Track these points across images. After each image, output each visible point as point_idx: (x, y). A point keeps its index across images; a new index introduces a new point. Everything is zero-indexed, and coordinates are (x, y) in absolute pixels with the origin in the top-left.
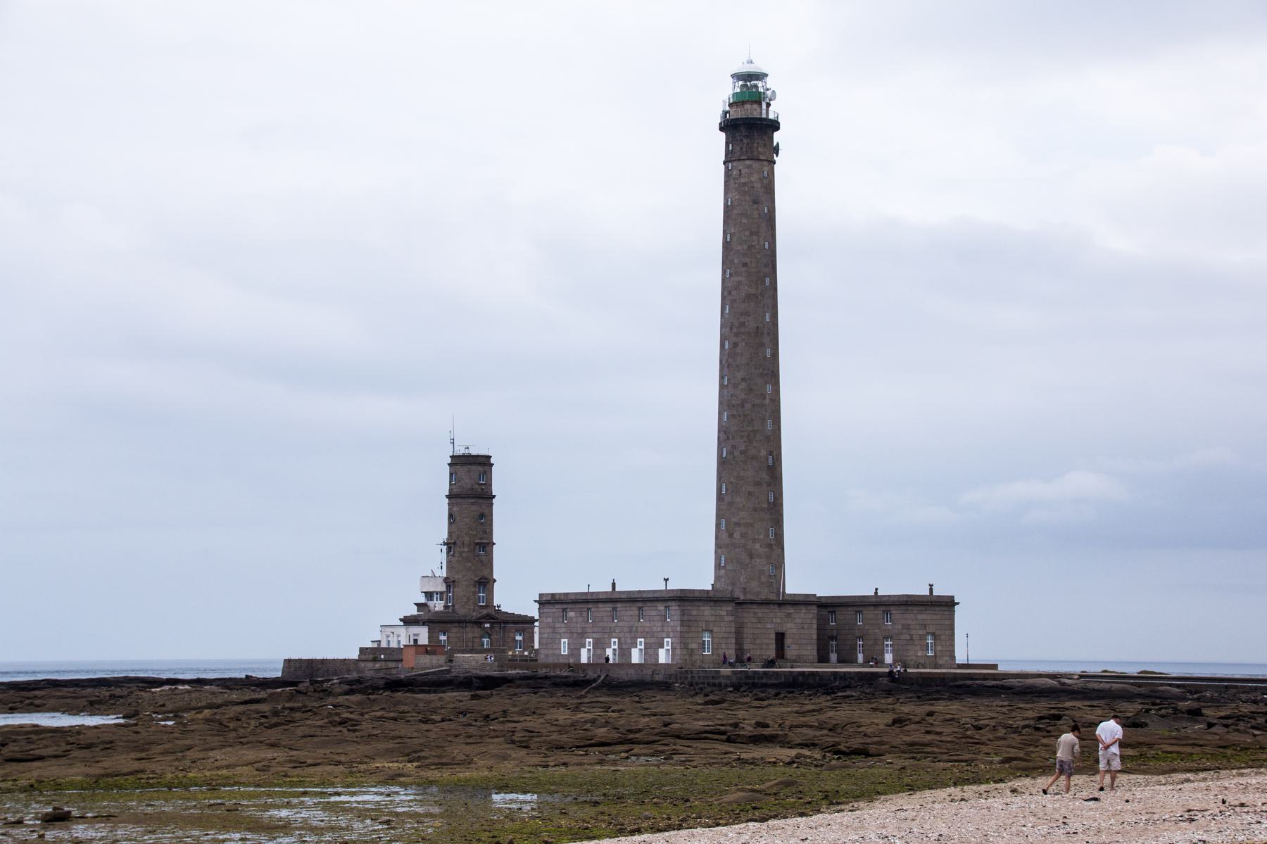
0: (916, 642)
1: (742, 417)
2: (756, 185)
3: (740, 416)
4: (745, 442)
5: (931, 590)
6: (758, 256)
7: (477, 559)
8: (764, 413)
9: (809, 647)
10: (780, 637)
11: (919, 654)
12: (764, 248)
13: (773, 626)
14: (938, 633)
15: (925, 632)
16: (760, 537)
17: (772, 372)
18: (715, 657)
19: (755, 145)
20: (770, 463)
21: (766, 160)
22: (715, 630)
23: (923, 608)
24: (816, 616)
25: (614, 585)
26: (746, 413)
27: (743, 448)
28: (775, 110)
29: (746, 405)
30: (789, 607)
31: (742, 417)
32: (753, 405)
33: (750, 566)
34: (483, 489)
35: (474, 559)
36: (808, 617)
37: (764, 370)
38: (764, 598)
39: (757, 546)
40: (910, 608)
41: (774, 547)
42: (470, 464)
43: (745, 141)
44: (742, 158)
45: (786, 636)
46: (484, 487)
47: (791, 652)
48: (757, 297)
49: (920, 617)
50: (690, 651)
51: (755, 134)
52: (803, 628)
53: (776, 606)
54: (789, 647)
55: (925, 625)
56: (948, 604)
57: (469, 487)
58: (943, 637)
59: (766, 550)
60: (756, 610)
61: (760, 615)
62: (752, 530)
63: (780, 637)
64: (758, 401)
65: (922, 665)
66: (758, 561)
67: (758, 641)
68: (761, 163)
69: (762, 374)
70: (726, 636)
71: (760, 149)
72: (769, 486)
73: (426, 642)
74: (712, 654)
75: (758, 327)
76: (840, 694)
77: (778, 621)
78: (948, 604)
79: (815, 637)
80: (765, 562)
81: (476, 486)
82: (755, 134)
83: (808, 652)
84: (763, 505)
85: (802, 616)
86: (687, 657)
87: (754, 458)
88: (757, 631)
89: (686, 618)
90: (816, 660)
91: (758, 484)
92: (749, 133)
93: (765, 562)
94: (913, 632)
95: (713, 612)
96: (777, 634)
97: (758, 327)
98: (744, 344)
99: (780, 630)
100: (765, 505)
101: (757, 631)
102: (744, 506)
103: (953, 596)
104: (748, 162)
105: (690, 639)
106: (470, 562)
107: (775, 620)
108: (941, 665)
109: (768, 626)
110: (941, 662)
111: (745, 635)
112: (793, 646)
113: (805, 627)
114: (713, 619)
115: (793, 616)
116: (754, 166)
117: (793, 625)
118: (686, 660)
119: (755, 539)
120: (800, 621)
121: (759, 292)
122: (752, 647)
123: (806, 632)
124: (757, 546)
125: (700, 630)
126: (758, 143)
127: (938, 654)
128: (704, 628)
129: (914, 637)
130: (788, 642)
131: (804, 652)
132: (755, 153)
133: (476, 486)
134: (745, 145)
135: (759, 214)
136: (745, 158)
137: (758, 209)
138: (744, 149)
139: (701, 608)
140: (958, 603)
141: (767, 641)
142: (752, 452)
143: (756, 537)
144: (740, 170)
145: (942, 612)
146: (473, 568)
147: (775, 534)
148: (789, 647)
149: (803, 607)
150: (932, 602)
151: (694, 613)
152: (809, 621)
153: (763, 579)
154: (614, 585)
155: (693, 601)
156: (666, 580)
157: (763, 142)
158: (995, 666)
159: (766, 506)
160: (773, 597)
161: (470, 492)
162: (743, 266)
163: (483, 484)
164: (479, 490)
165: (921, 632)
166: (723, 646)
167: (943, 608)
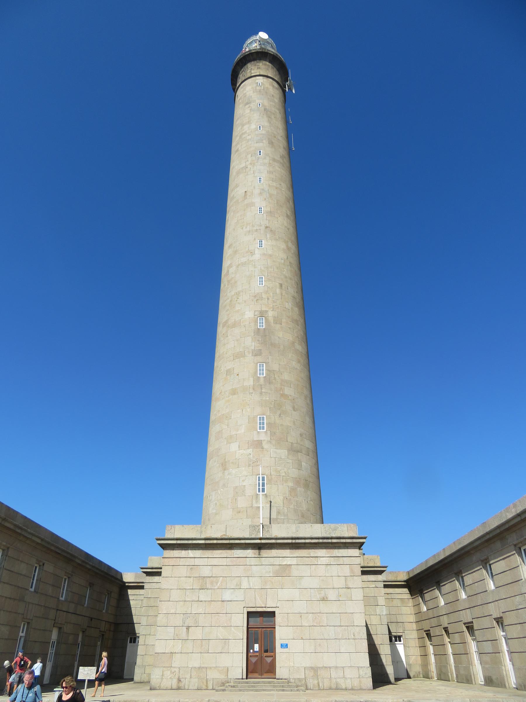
13: (239, 595)
16: (239, 432)
30: (287, 552)
37: (253, 226)
41: (266, 446)
45: (278, 619)
52: (324, 599)
53: (250, 552)
59: (250, 451)
60: (197, 562)
61: (206, 571)
67: (196, 633)
69: (249, 231)
72: (256, 355)
73: (258, 650)
77: (255, 583)
85: (321, 571)
88: (196, 609)
99: (260, 606)
100: (250, 382)
101: (196, 609)
109: (227, 595)
111: (161, 619)
115: (295, 572)
119: (231, 437)
120: (315, 583)
122: (178, 646)
123: (334, 608)
124: (234, 447)
131: (328, 660)
141: (221, 633)
152: (340, 583)
153: (242, 503)
159: (251, 382)
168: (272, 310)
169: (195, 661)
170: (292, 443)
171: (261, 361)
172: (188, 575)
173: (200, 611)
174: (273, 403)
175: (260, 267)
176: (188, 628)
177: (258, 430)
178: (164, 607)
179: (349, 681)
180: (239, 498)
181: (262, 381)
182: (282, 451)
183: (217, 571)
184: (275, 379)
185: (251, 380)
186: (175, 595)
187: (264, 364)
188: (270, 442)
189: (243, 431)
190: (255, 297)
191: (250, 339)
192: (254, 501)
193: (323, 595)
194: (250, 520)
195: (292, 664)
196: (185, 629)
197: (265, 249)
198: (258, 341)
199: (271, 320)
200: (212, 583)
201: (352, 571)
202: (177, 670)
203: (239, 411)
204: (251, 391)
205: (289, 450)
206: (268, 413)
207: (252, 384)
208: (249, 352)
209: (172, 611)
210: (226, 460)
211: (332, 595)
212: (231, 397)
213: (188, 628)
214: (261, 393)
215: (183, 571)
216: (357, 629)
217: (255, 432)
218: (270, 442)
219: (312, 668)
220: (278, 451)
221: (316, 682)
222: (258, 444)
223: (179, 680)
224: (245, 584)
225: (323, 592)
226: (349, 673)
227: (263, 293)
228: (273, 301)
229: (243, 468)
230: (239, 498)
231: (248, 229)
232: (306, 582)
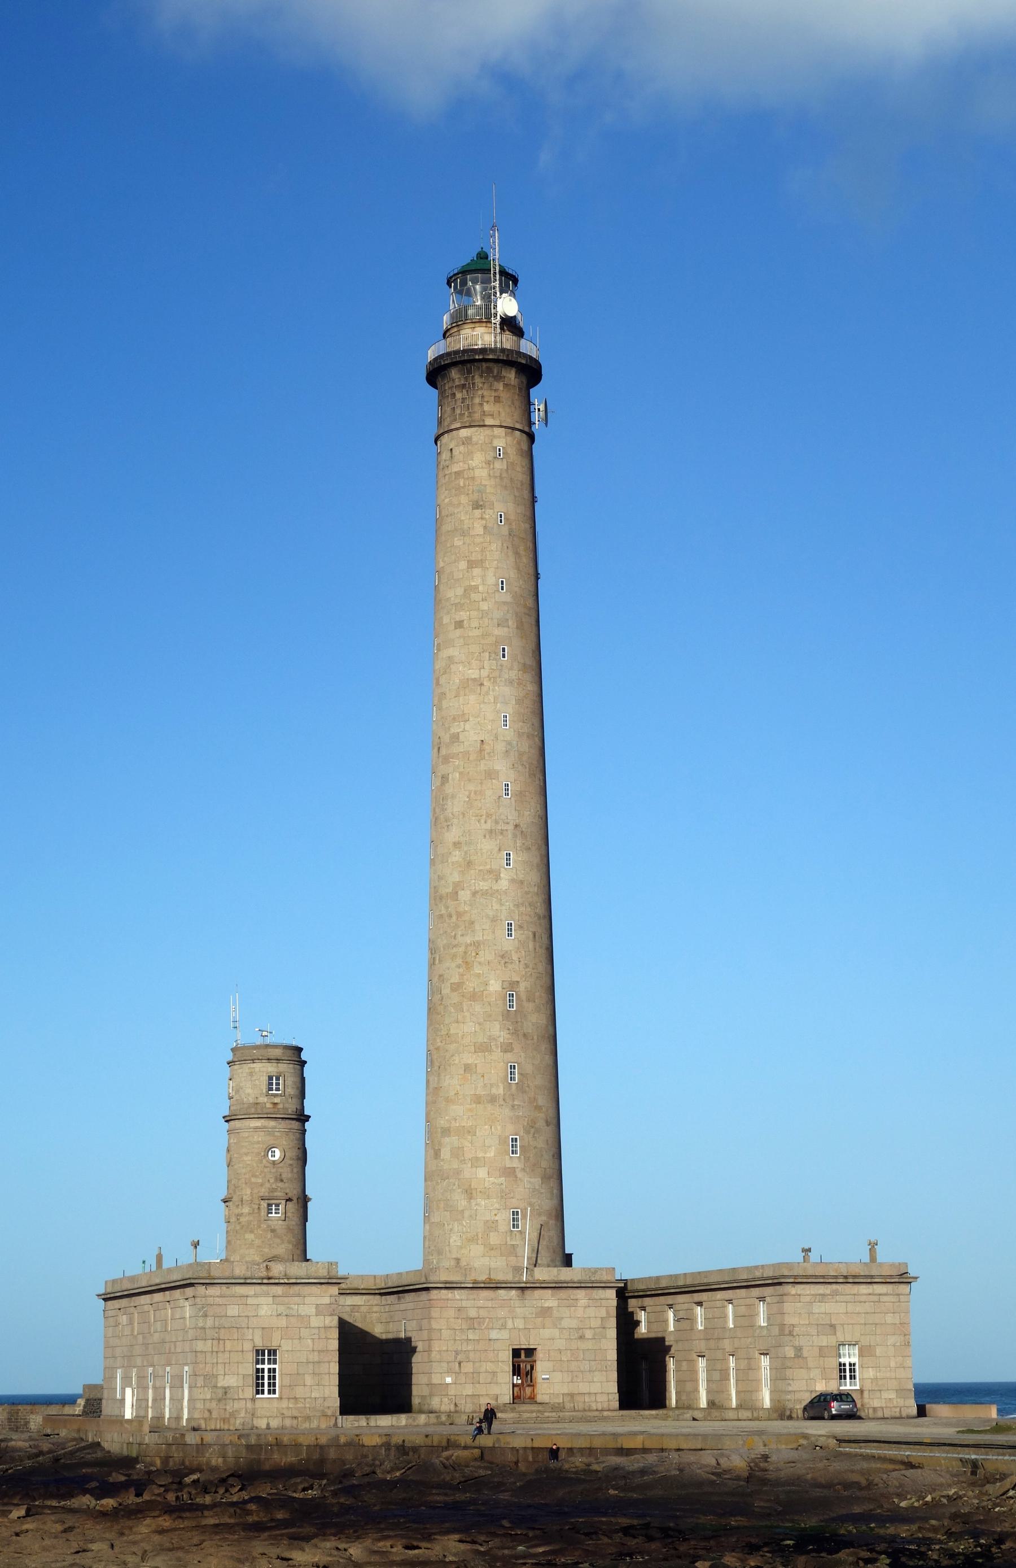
0: (811, 1364)
1: (454, 918)
2: (478, 473)
3: (450, 916)
4: (459, 966)
6: (484, 606)
7: (264, 1226)
8: (496, 906)
9: (598, 1377)
14: (865, 1341)
15: (832, 1341)
16: (488, 1155)
17: (516, 826)
18: (284, 1404)
19: (477, 400)
21: (501, 426)
22: (286, 1346)
25: (159, 1258)
26: (461, 909)
27: (455, 979)
29: (461, 893)
31: (454, 918)
32: (474, 894)
33: (467, 1214)
34: (275, 1104)
35: (259, 1227)
37: (497, 822)
39: (482, 1173)
41: (520, 1175)
42: (253, 1061)
43: (459, 396)
44: (453, 427)
45: (539, 1355)
46: (277, 1100)
48: (482, 685)
49: (818, 1308)
50: (220, 1392)
51: (478, 380)
52: (582, 1337)
55: (833, 1326)
57: (251, 1100)
58: (879, 1351)
60: (464, 1304)
61: (473, 1313)
62: (471, 1143)
64: (483, 885)
66: (483, 1203)
67: (468, 1368)
68: (488, 431)
69: (491, 831)
70: (316, 1359)
71: (486, 407)
72: (506, 1052)
74: (280, 1398)
76: (54, 1503)
77: (520, 1323)
79: (612, 1355)
80: (497, 1206)
81: (263, 1099)
82: (478, 380)
83: (595, 1388)
84: (494, 1091)
85: (580, 1312)
86: (214, 1404)
87: (474, 997)
89: (209, 1322)
90: (617, 1404)
91: (482, 1048)
92: (466, 379)
93: (497, 1206)
94: (802, 1341)
95: (281, 1309)
96: (516, 1353)
97: (482, 741)
98: (457, 775)
100: (500, 1091)
102: (457, 1094)
103: (906, 1265)
104: (464, 433)
105: (220, 1367)
106: (252, 1232)
108: (875, 1409)
109: (494, 1334)
110: (876, 1403)
112: (558, 1376)
113: (587, 1336)
114: (283, 1322)
115: (555, 1313)
116: (475, 439)
117: (556, 1332)
118: (210, 1411)
119: (477, 1159)
120: (574, 1323)
121: (485, 673)
123: (589, 1345)
124: (482, 1173)
125: (248, 1346)
126: (483, 397)
127: (868, 1386)
129: (805, 1353)
131: (583, 1388)
132: (477, 416)
133: (265, 1099)
134: (459, 403)
135: (485, 527)
136: (458, 425)
137: (482, 518)
138: (458, 411)
139: (250, 1301)
141: (490, 1367)
142: (470, 985)
143: (480, 1155)
144: (451, 450)
145: (876, 1298)
146: (257, 1242)
149: (581, 1294)
150: (846, 1277)
151: (233, 1311)
152: (596, 1323)
153: (494, 1239)
154: (159, 1258)
157: (494, 394)
159: (501, 1091)
161: (253, 1110)
162: (456, 628)
163: (275, 1095)
164: (269, 1105)
165: (824, 1341)
166: (309, 1380)
168: (524, 979)
169: (469, 1390)
170: (545, 1169)
171: (512, 1061)
172: (456, 1316)
173: (470, 1348)
174: (526, 1119)
175: (508, 904)
176: (460, 1364)
177: (511, 1155)
178: (436, 1346)
179: (600, 1404)
180: (492, 1234)
181: (514, 1087)
182: (536, 1180)
183: (483, 1313)
184: (528, 1087)
185: (501, 1086)
186: (446, 1334)
187: (516, 1064)
188: (523, 1170)
189: (492, 1154)
190: (503, 957)
191: (497, 1026)
192: (508, 1238)
193: (580, 1334)
194: (505, 1258)
195: (552, 1392)
197: (514, 871)
198: (509, 1029)
199: (523, 996)
200: (479, 1323)
201: (608, 1312)
202: (453, 1397)
203: (486, 1127)
204: (502, 1103)
205: (542, 1179)
206: (522, 1134)
207: (502, 1093)
208: (497, 1047)
209: (444, 1348)
210: (472, 1187)
211: (589, 1334)
212: (474, 1105)
213: (460, 1364)
214: (513, 1106)
215: (451, 1313)
216: (609, 1363)
217: (507, 1157)
218: (523, 1170)
219: (568, 1394)
220: (532, 1180)
221: (572, 1405)
223: (456, 1405)
224: (510, 1324)
225: (581, 1331)
226: (599, 1398)
227: (513, 952)
228: (526, 964)
229: (495, 1200)
230: (492, 1234)
231: (488, 826)
232: (565, 1323)
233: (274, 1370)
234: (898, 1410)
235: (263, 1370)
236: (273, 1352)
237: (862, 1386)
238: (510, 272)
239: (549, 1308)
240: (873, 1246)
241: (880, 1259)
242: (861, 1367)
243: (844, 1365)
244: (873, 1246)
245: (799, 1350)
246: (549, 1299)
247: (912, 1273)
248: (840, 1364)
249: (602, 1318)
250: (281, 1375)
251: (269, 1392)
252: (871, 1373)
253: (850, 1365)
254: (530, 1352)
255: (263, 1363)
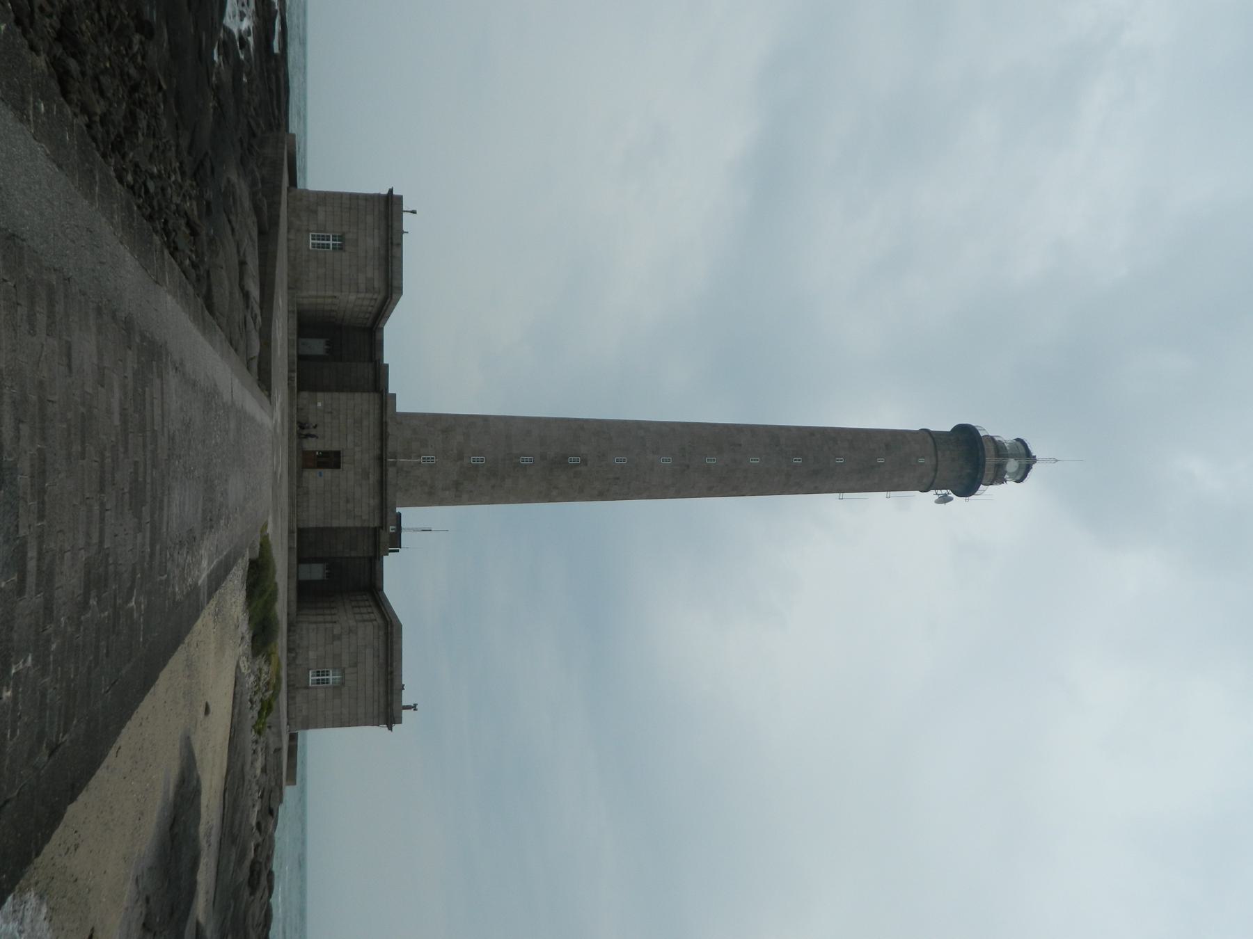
5: (408, 708)
10: (331, 460)
11: (312, 654)
12: (836, 457)
17: (688, 466)
20: (572, 460)
21: (937, 461)
23: (382, 655)
24: (366, 524)
28: (989, 494)
36: (363, 513)
38: (389, 430)
40: (382, 633)
45: (336, 471)
47: (317, 479)
52: (347, 501)
53: (377, 452)
54: (320, 475)
55: (355, 665)
56: (389, 714)
61: (365, 423)
63: (331, 460)
65: (295, 658)
74: (309, 250)
75: (740, 445)
78: (389, 714)
79: (335, 524)
90: (301, 526)
96: (337, 454)
103: (401, 722)
107: (358, 451)
108: (294, 698)
109: (350, 438)
111: (336, 395)
118: (301, 200)
128: (348, 236)
130: (328, 473)
139: (376, 231)
140: (390, 729)
147: (477, 465)
148: (320, 475)
150: (392, 673)
155: (387, 218)
156: (414, 212)
158: (292, 779)
160: (392, 445)
167: (382, 701)
176: (331, 413)
196: (330, 410)
213: (331, 413)
222: (460, 457)
223: (302, 409)
224: (357, 449)
233: (328, 248)
234: (294, 716)
235: (328, 240)
236: (341, 248)
237: (311, 688)
238: (1029, 474)
239: (369, 478)
240: (414, 707)
241: (404, 712)
242: (327, 687)
243: (327, 675)
244: (414, 707)
245: (339, 637)
246: (373, 478)
247: (396, 727)
248: (327, 671)
249: (361, 516)
250: (325, 252)
251: (313, 244)
252: (321, 695)
253: (327, 679)
254: (337, 465)
255: (333, 240)
